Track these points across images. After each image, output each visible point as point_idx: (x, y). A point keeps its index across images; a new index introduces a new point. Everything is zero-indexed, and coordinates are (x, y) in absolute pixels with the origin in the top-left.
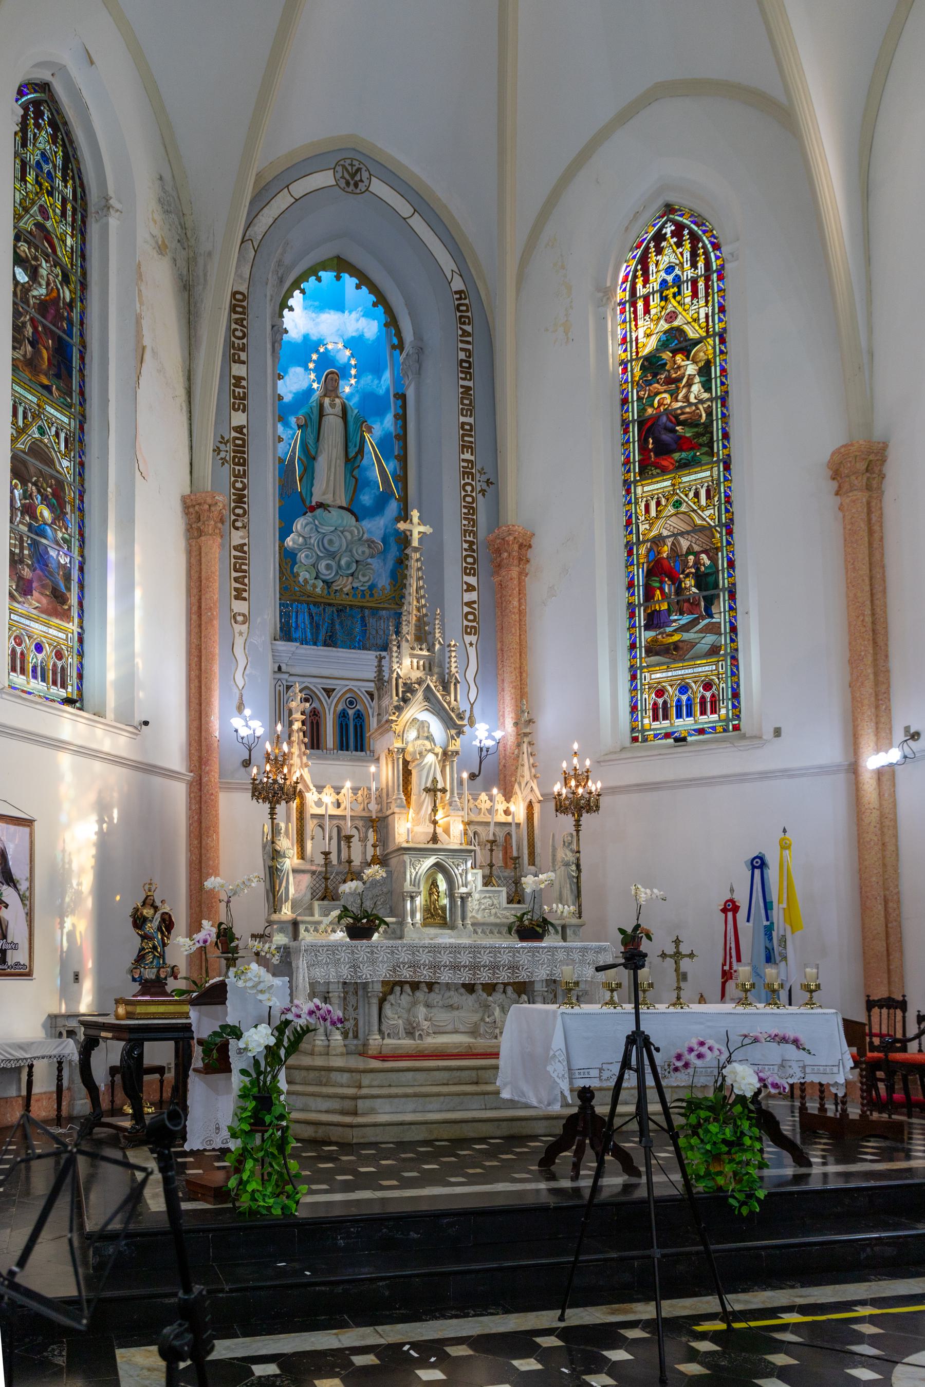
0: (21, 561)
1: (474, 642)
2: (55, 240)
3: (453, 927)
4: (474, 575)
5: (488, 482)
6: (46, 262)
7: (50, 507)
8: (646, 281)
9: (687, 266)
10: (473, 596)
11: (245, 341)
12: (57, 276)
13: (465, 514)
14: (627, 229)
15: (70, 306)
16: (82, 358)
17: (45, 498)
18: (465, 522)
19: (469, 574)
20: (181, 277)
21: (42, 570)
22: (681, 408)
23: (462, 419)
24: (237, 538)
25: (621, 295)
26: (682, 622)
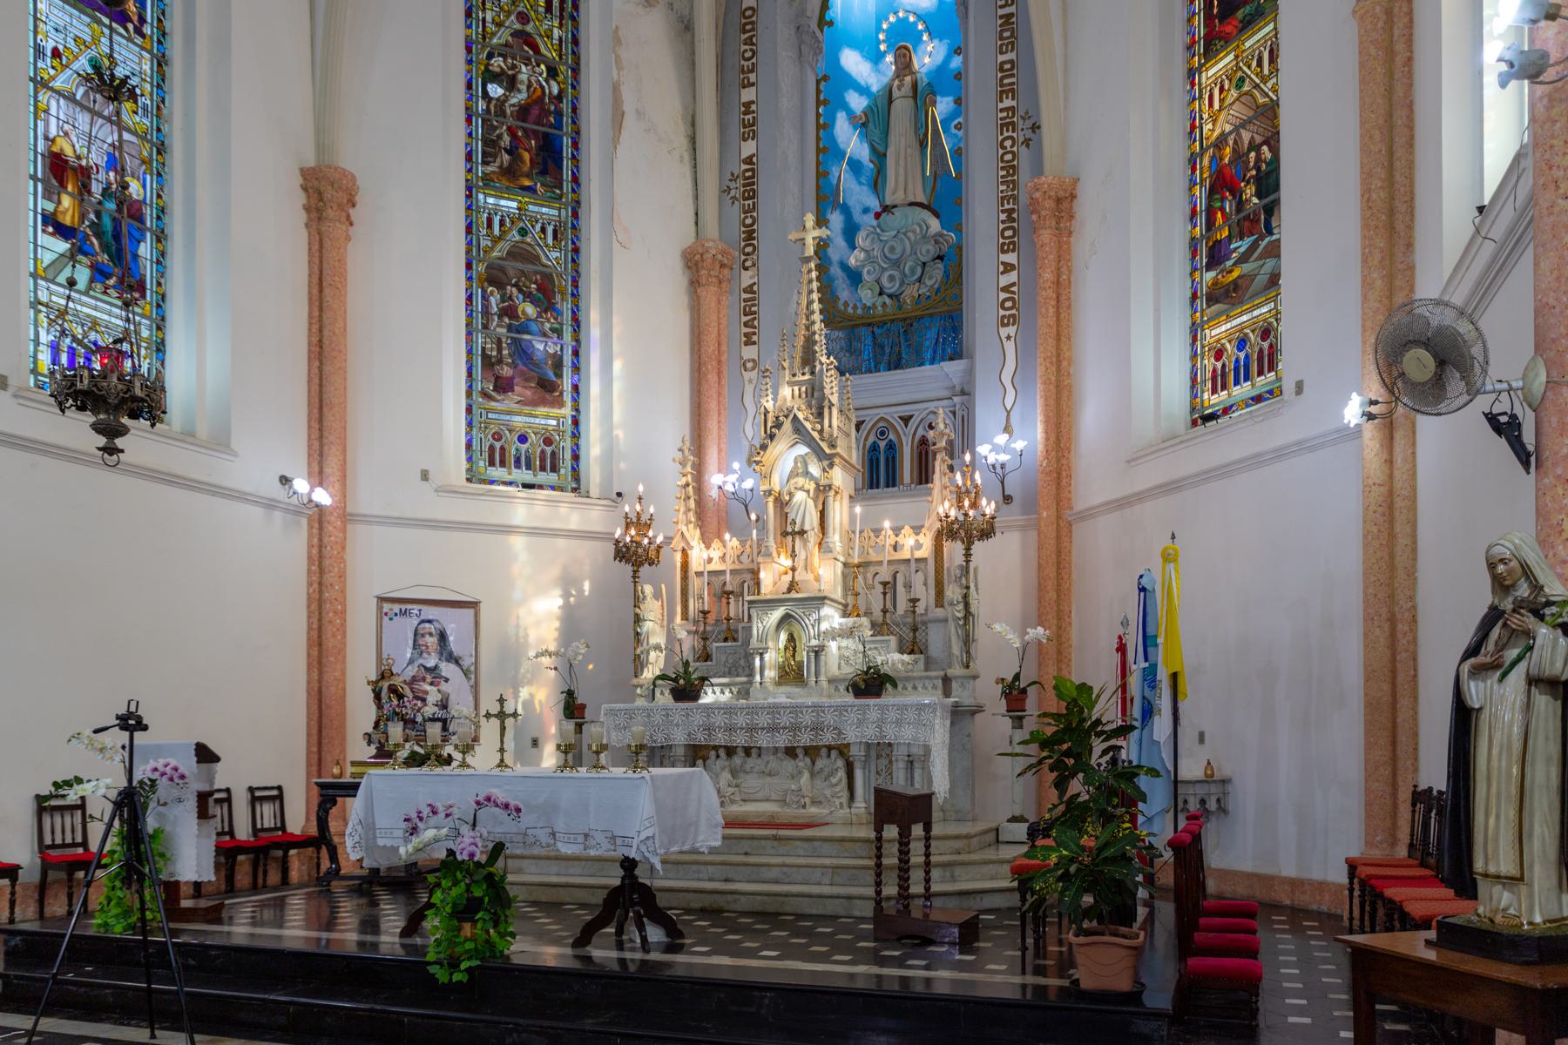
0: (500, 361)
1: (1013, 334)
2: (538, 40)
4: (1013, 251)
6: (526, 65)
7: (535, 302)
10: (1012, 277)
11: (754, 60)
12: (541, 75)
13: (1002, 177)
15: (559, 98)
16: (575, 145)
17: (528, 296)
18: (1001, 188)
19: (1004, 252)
20: (681, 19)
21: (525, 365)
23: (1001, 58)
26: (1242, 250)
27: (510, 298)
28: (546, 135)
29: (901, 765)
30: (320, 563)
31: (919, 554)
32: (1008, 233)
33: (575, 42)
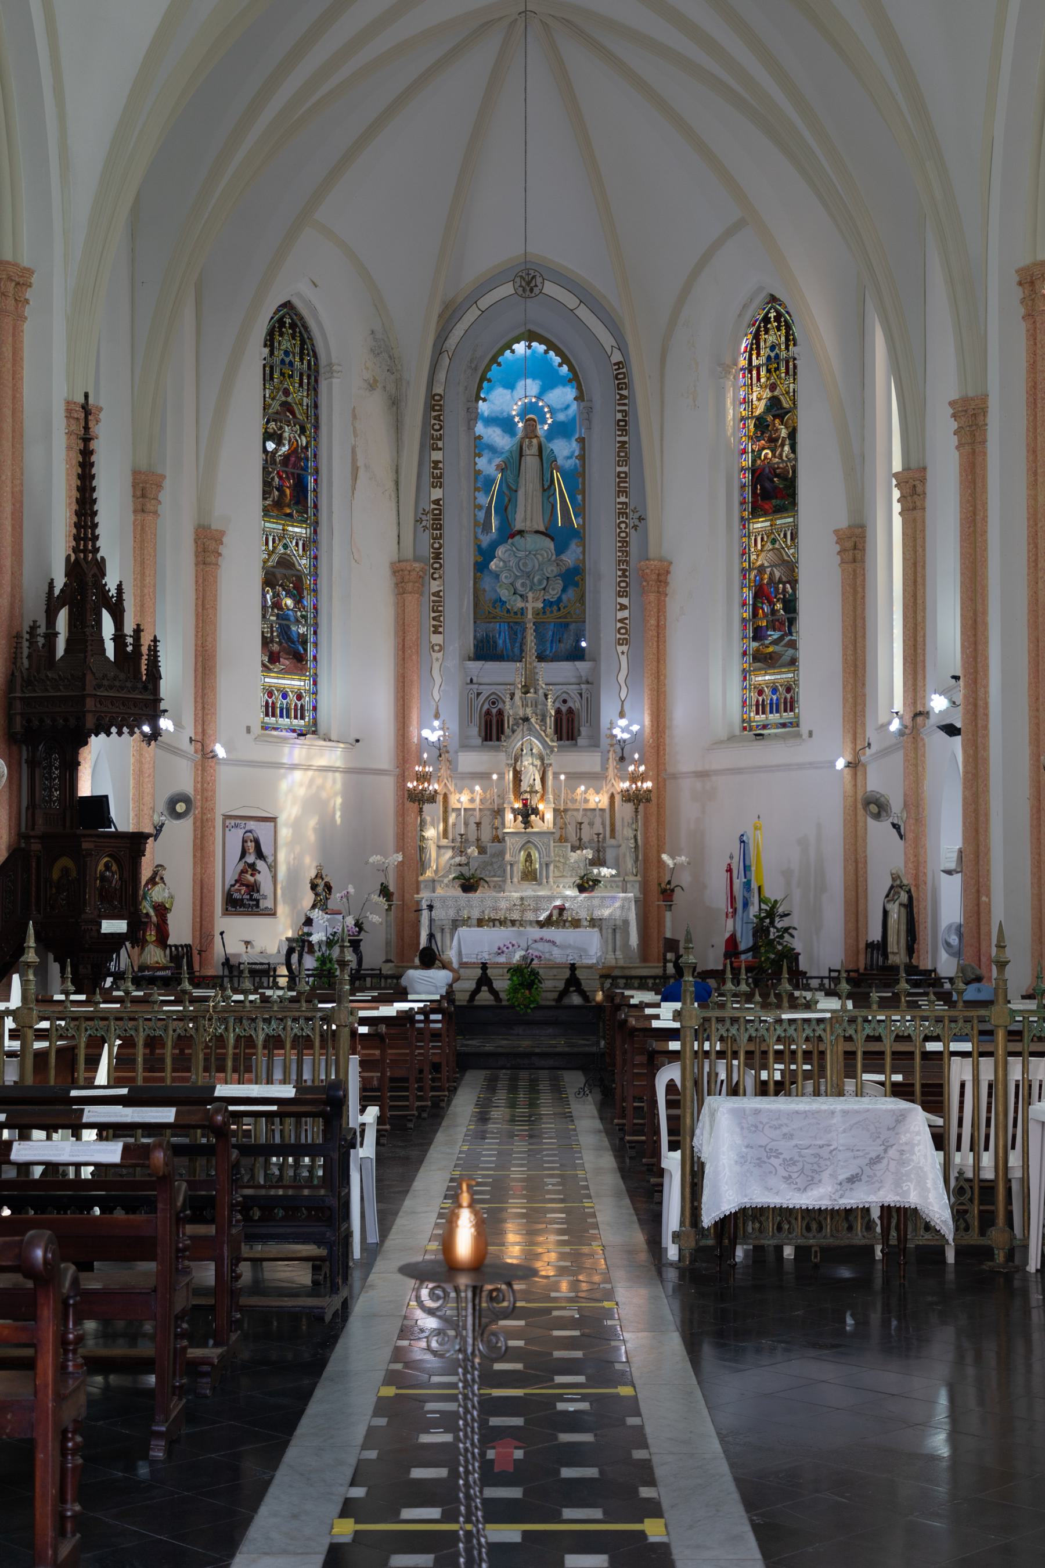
0: (272, 641)
3: (540, 884)
5: (640, 519)
8: (758, 355)
9: (783, 347)
10: (625, 614)
14: (740, 315)
15: (306, 448)
17: (289, 594)
19: (620, 596)
22: (778, 463)
23: (619, 469)
24: (435, 586)
25: (743, 362)
26: (775, 637)
27: (278, 595)
28: (298, 475)
29: (610, 931)
30: (202, 793)
31: (600, 806)
32: (623, 584)
33: (316, 406)
